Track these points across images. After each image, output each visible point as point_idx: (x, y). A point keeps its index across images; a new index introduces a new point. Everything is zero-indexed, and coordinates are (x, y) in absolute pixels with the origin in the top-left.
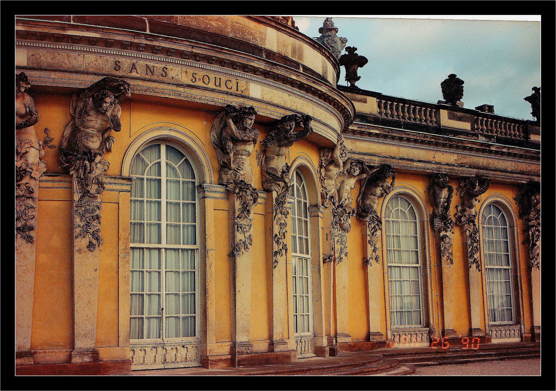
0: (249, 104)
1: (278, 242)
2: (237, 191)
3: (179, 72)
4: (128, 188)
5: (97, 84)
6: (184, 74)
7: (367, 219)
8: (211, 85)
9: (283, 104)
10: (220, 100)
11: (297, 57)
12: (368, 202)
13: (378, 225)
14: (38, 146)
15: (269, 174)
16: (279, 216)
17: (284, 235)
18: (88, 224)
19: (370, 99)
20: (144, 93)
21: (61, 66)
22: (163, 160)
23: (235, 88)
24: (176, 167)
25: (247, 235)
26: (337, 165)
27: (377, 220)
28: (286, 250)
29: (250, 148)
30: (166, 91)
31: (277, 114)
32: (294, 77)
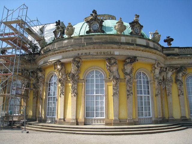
0: (113, 56)
7: (178, 83)
9: (127, 55)
16: (129, 85)
18: (74, 91)
19: (175, 49)
22: (95, 74)
23: (110, 53)
32: (128, 47)
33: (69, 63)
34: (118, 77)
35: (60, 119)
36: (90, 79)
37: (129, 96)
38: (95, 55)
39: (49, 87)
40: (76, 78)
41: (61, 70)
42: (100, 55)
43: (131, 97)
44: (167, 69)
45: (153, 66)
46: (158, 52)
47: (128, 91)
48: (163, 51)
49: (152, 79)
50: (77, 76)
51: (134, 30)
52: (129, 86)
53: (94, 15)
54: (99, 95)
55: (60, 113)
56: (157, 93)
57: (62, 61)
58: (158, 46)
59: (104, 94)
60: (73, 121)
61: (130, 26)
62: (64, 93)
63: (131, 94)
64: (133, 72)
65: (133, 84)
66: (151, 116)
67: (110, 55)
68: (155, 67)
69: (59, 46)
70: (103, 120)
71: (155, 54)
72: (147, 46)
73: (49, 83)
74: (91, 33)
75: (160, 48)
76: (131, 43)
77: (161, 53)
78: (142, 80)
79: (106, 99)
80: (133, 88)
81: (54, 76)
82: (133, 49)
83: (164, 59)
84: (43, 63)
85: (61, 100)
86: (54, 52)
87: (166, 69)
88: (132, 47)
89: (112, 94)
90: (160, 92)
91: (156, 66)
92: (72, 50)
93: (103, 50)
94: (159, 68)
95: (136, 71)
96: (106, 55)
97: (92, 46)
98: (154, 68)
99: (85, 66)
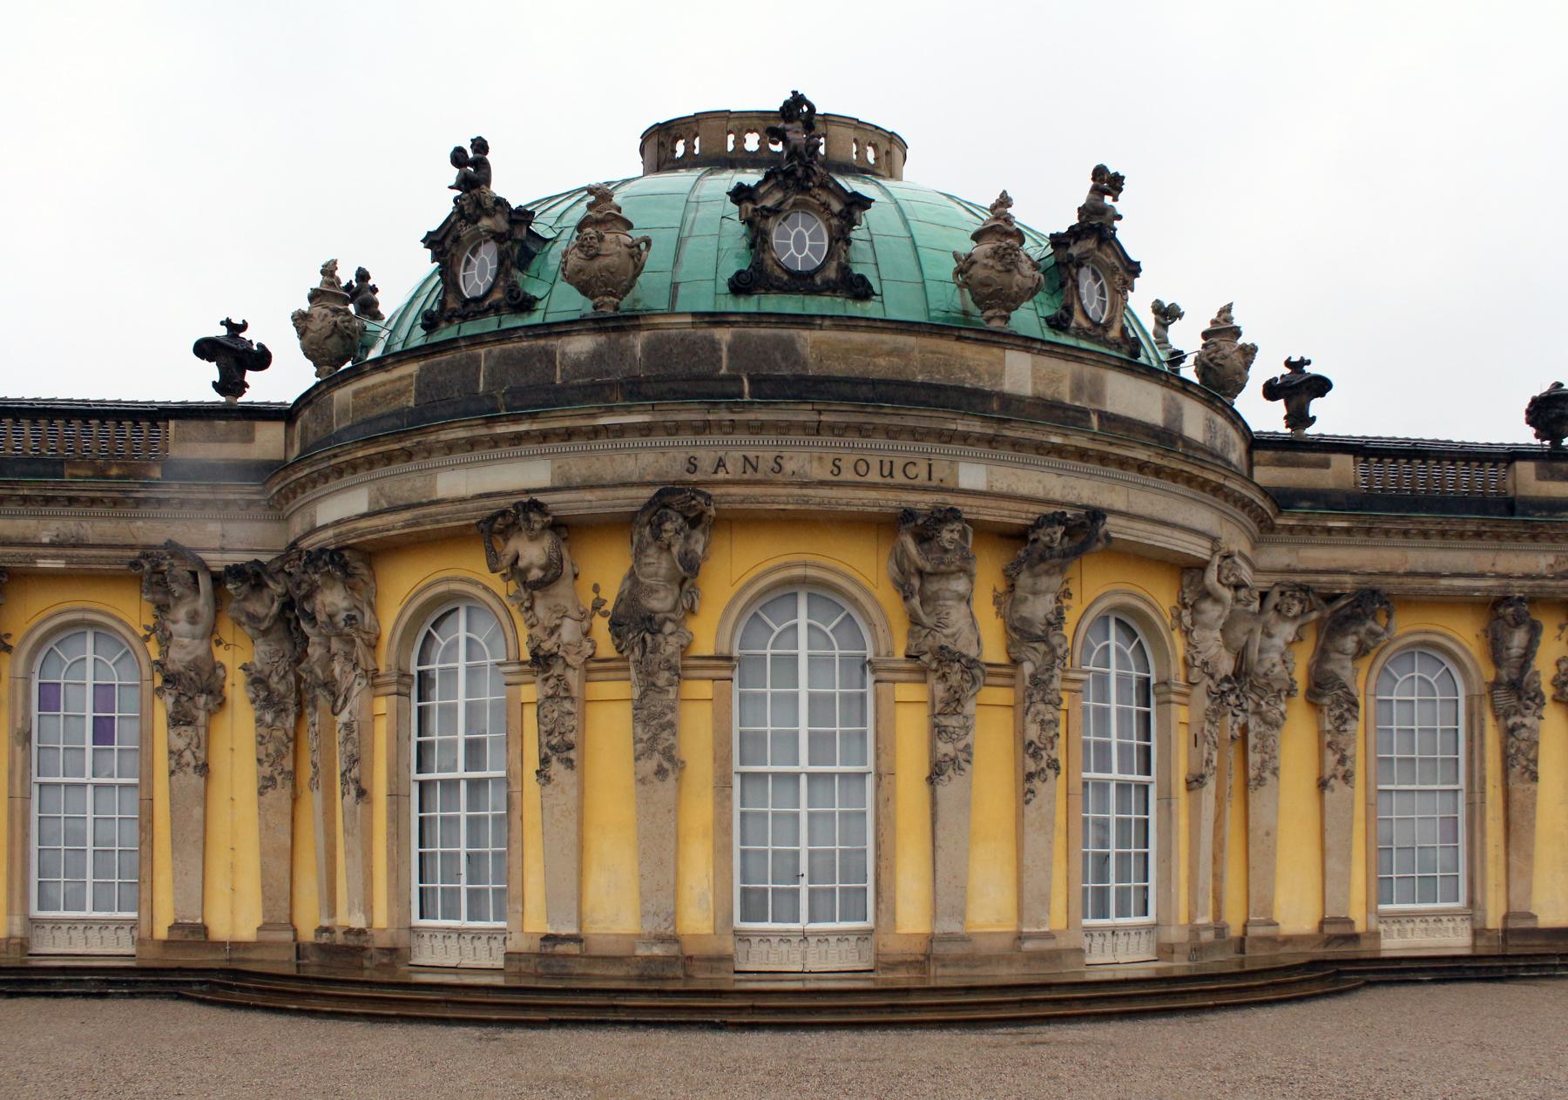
0: (952, 500)
1: (1035, 755)
2: (934, 665)
5: (651, 503)
6: (815, 464)
8: (874, 477)
10: (892, 501)
12: (1329, 667)
13: (1348, 710)
14: (577, 615)
15: (1015, 629)
16: (1041, 707)
17: (1052, 742)
18: (654, 738)
20: (738, 506)
21: (602, 478)
22: (802, 620)
23: (922, 478)
24: (827, 630)
25: (961, 745)
26: (1218, 600)
27: (1348, 701)
28: (1057, 769)
29: (960, 585)
30: (783, 497)
31: (1020, 516)
34: (973, 653)
35: (547, 938)
36: (769, 652)
37: (1037, 783)
40: (670, 650)
44: (1275, 598)
54: (832, 775)
55: (551, 898)
59: (870, 766)
60: (658, 950)
63: (1050, 773)
64: (1066, 614)
67: (925, 490)
80: (1061, 730)
83: (1254, 527)
84: (363, 507)
87: (1264, 596)
93: (877, 451)
95: (1087, 610)
99: (735, 567)
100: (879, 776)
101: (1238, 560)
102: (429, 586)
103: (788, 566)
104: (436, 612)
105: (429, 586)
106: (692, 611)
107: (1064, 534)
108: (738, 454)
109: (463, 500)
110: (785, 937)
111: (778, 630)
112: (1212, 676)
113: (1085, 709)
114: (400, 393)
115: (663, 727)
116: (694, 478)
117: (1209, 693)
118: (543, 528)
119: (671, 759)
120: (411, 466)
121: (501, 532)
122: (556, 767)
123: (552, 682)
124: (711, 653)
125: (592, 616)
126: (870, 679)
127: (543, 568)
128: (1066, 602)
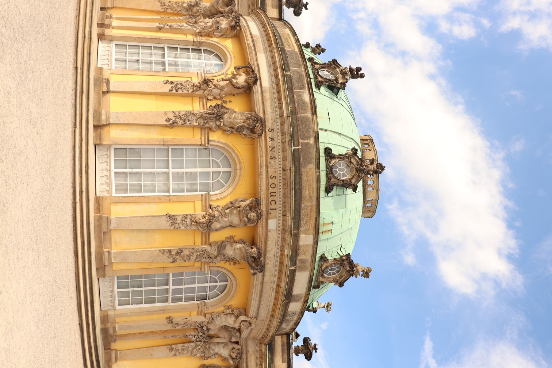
0: (264, 217)
1: (177, 252)
2: (208, 213)
3: (276, 167)
4: (203, 143)
6: (274, 170)
9: (268, 249)
10: (263, 196)
11: (300, 264)
15: (222, 243)
16: (195, 254)
18: (180, 117)
22: (222, 170)
23: (272, 207)
24: (219, 178)
26: (235, 322)
28: (173, 262)
32: (286, 252)
33: (251, 107)
35: (108, 82)
37: (168, 255)
38: (267, 172)
39: (190, 47)
41: (233, 85)
42: (267, 183)
43: (166, 260)
45: (242, 310)
46: (275, 323)
47: (180, 252)
48: (281, 335)
49: (211, 310)
50: (219, 127)
51: (331, 266)
52: (193, 253)
53: (371, 167)
56: (175, 321)
57: (257, 89)
58: (292, 324)
59: (172, 194)
60: (104, 117)
61: (341, 255)
62: (174, 91)
63: (171, 260)
64: (228, 263)
65: (197, 264)
66: (118, 307)
67: (267, 208)
68: (241, 315)
69: (294, 79)
70: (110, 191)
71: (272, 316)
72: (289, 296)
73: (202, 48)
74: (327, 160)
75: (286, 327)
76: (296, 259)
77: (272, 331)
78: (208, 285)
79: (159, 198)
80: (187, 264)
81: (219, 62)
82: (281, 263)
84: (253, 33)
85: (156, 83)
86: (278, 66)
88: (287, 261)
89: (171, 213)
90: (177, 328)
91: (242, 318)
92: (281, 116)
93: (279, 191)
94: (237, 326)
96: (267, 199)
97: (289, 164)
98: (236, 312)
99: (239, 146)
100: (168, 196)
101: (250, 328)
102: (229, 52)
103: (240, 163)
104: (221, 56)
105: (229, 52)
106: (224, 131)
107: (255, 258)
108: (275, 145)
109: (257, 61)
110: (109, 164)
111: (218, 161)
112: (208, 323)
113: (194, 274)
114: (289, 46)
115: (184, 120)
116: (267, 130)
117: (203, 322)
118: (248, 84)
119: (173, 123)
120: (267, 46)
121: (247, 71)
122: (169, 86)
123: (198, 85)
124: (210, 138)
125: (221, 100)
126: (204, 193)
127: (236, 83)
128: (232, 263)
